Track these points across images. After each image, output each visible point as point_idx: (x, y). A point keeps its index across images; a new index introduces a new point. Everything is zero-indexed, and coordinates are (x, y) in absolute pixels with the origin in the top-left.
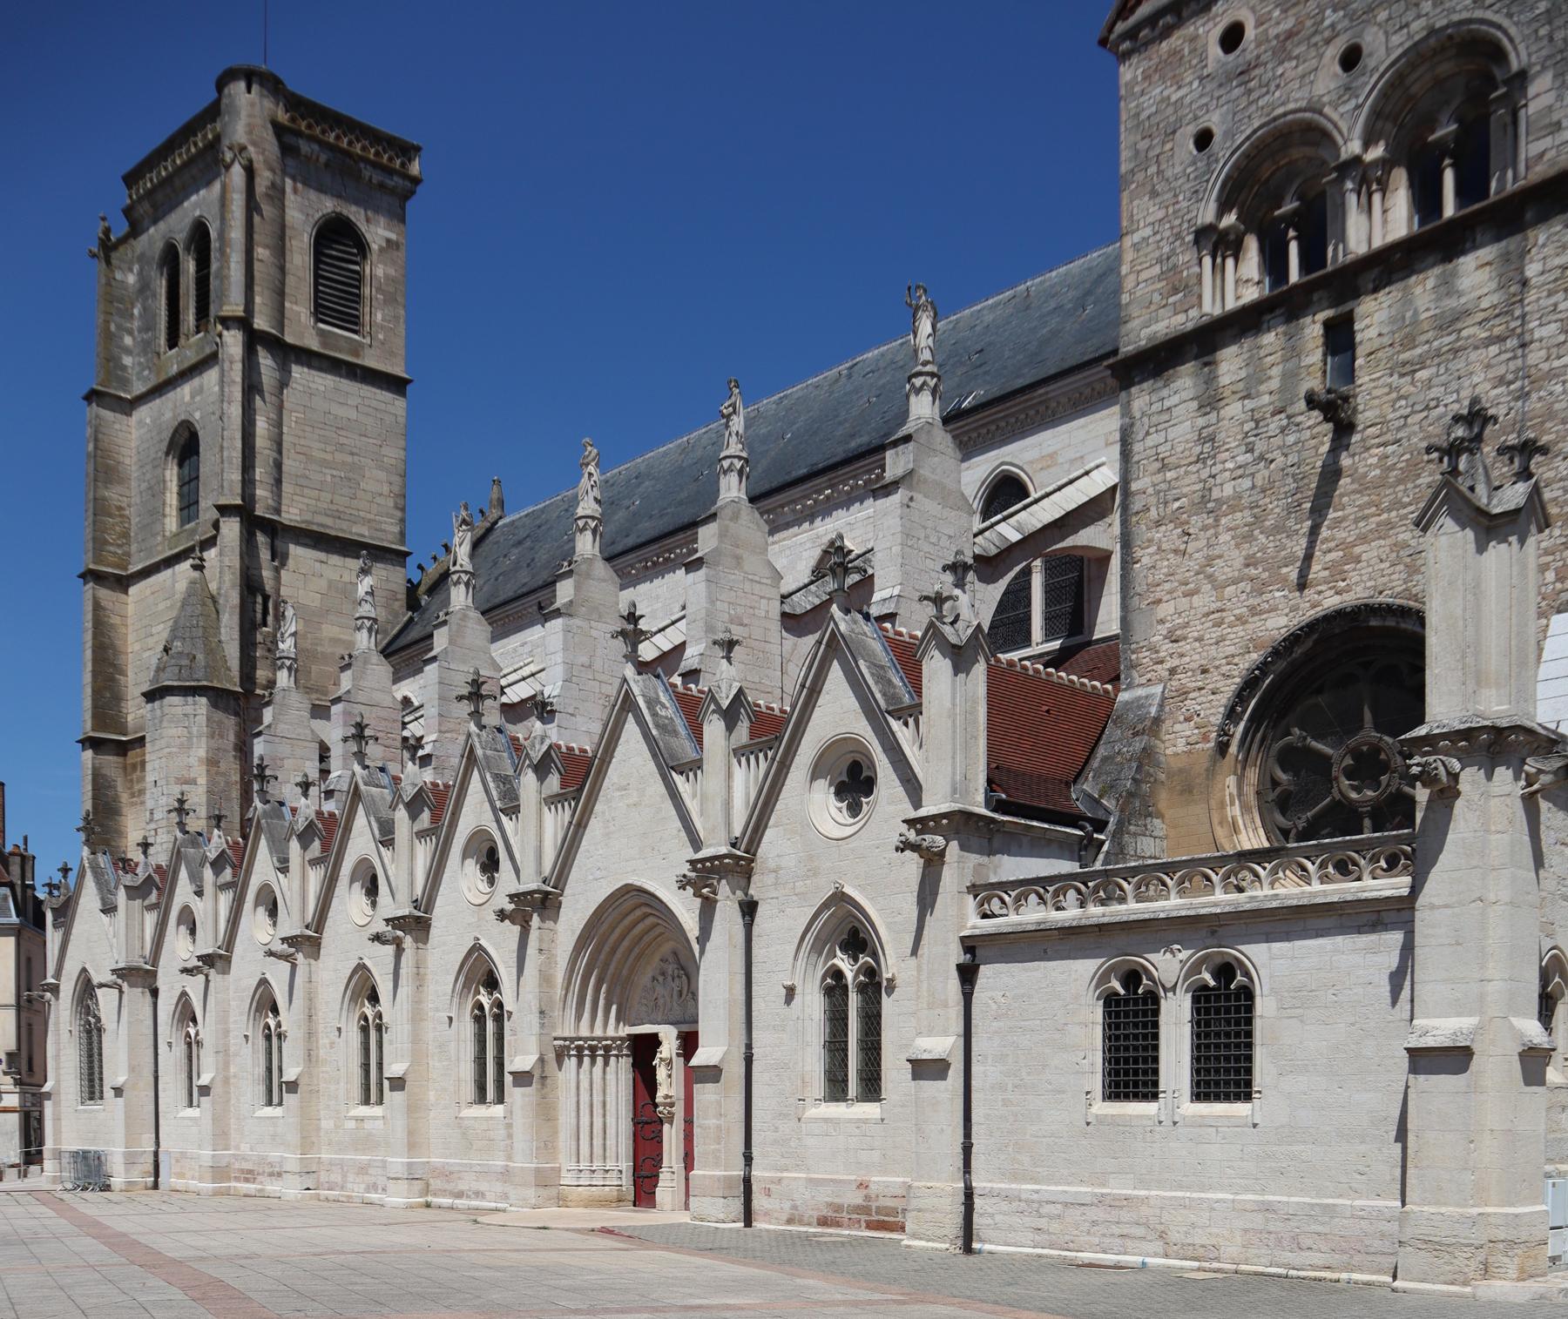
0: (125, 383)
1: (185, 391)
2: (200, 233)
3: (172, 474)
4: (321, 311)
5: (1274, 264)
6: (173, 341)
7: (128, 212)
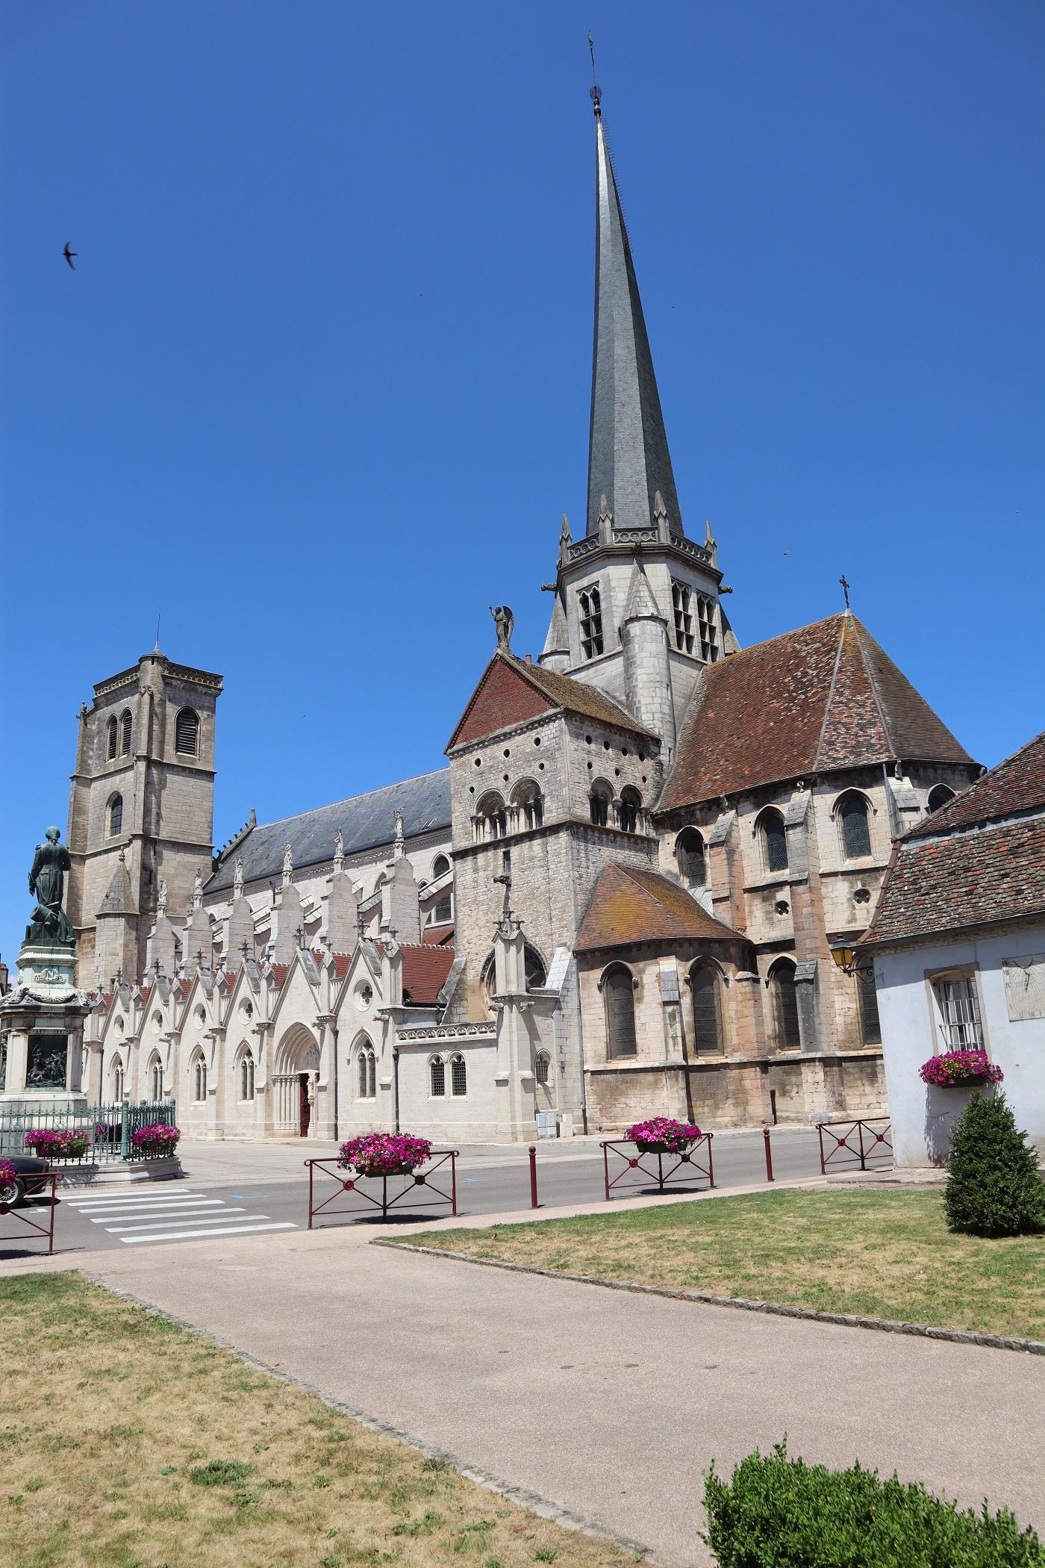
7: (94, 700)
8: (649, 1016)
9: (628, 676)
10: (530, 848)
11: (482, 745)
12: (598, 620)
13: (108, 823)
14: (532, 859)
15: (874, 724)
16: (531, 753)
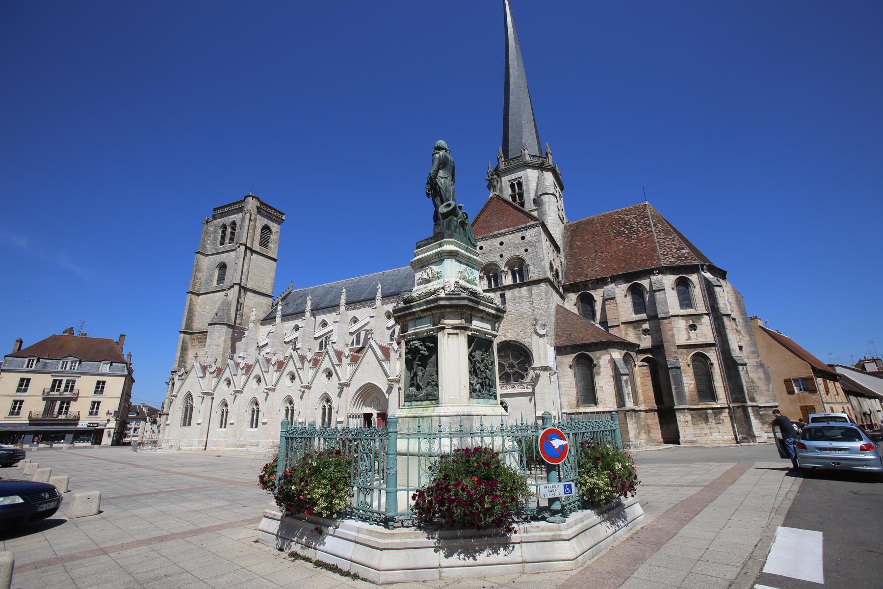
0: (206, 251)
1: (224, 255)
2: (234, 224)
3: (217, 273)
4: (261, 244)
5: (490, 282)
6: (222, 243)
8: (604, 383)
10: (520, 292)
11: (485, 239)
13: (216, 278)
14: (521, 298)
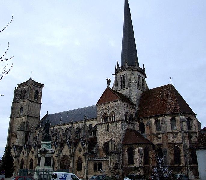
9: (130, 93)
12: (124, 82)
14: (113, 126)
15: (177, 106)
16: (114, 107)
